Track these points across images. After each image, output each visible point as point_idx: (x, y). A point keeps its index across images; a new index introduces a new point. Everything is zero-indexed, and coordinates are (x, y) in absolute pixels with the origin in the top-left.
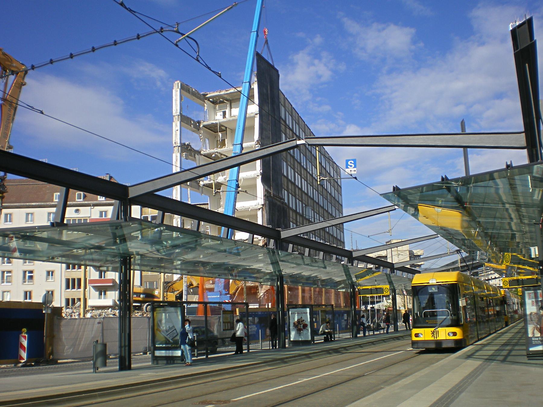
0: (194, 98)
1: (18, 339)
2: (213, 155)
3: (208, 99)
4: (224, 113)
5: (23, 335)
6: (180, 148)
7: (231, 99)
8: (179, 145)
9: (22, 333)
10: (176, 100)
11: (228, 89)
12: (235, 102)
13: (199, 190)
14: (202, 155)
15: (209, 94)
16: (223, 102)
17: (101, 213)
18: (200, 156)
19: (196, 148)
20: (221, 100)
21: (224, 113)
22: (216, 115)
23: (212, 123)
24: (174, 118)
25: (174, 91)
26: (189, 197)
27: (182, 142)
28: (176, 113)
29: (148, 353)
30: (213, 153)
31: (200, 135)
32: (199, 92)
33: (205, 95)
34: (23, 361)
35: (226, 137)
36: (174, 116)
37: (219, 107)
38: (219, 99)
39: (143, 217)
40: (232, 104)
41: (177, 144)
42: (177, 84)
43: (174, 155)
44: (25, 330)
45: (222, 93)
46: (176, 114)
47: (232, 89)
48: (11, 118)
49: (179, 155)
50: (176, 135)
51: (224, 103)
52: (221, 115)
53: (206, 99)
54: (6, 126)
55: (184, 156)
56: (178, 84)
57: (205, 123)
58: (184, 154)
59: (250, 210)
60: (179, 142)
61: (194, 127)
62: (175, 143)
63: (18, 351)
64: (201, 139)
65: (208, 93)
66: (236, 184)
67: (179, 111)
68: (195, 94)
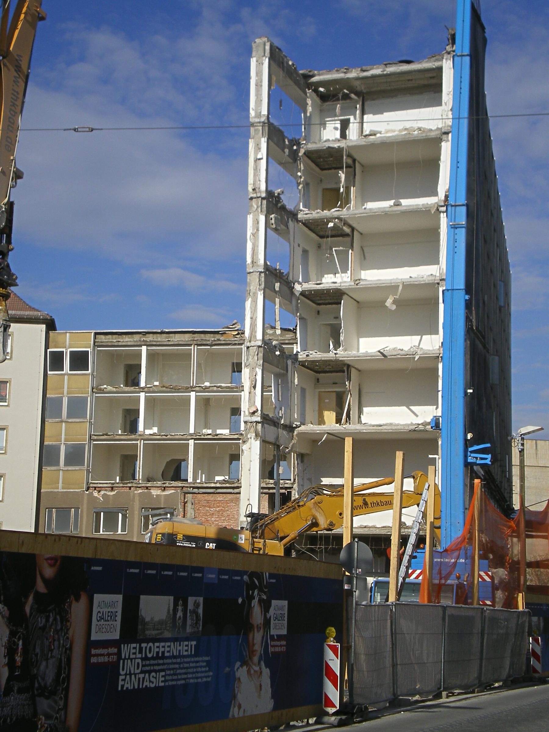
0: (290, 82)
1: (321, 654)
2: (331, 225)
3: (315, 87)
4: (345, 125)
5: (332, 643)
6: (265, 202)
7: (365, 91)
8: (264, 195)
9: (325, 638)
10: (259, 85)
11: (368, 68)
12: (373, 100)
13: (291, 302)
14: (300, 221)
15: (319, 75)
16: (346, 97)
18: (296, 223)
19: (290, 206)
20: (346, 91)
21: (345, 125)
22: (325, 129)
23: (329, 147)
24: (252, 129)
25: (253, 62)
26: (277, 318)
27: (269, 189)
28: (259, 115)
29: (444, 694)
30: (330, 220)
31: (299, 174)
32: (298, 69)
33: (307, 77)
34: (331, 710)
35: (354, 182)
36: (252, 125)
37: (342, 109)
38: (342, 90)
40: (366, 104)
41: (260, 192)
42: (262, 46)
43: (250, 219)
44: (332, 631)
45: (353, 74)
46: (257, 120)
47: (378, 68)
48: (19, 103)
49: (262, 218)
50: (257, 169)
51: (348, 101)
52: (336, 129)
53: (309, 86)
54: (9, 121)
55: (273, 221)
56: (265, 45)
57: (311, 146)
58: (272, 216)
59: (417, 358)
60: (263, 187)
61: (289, 156)
62: (254, 190)
63: (320, 686)
64: (299, 184)
65: (316, 72)
66: (466, 300)
67: (265, 112)
68: (290, 73)
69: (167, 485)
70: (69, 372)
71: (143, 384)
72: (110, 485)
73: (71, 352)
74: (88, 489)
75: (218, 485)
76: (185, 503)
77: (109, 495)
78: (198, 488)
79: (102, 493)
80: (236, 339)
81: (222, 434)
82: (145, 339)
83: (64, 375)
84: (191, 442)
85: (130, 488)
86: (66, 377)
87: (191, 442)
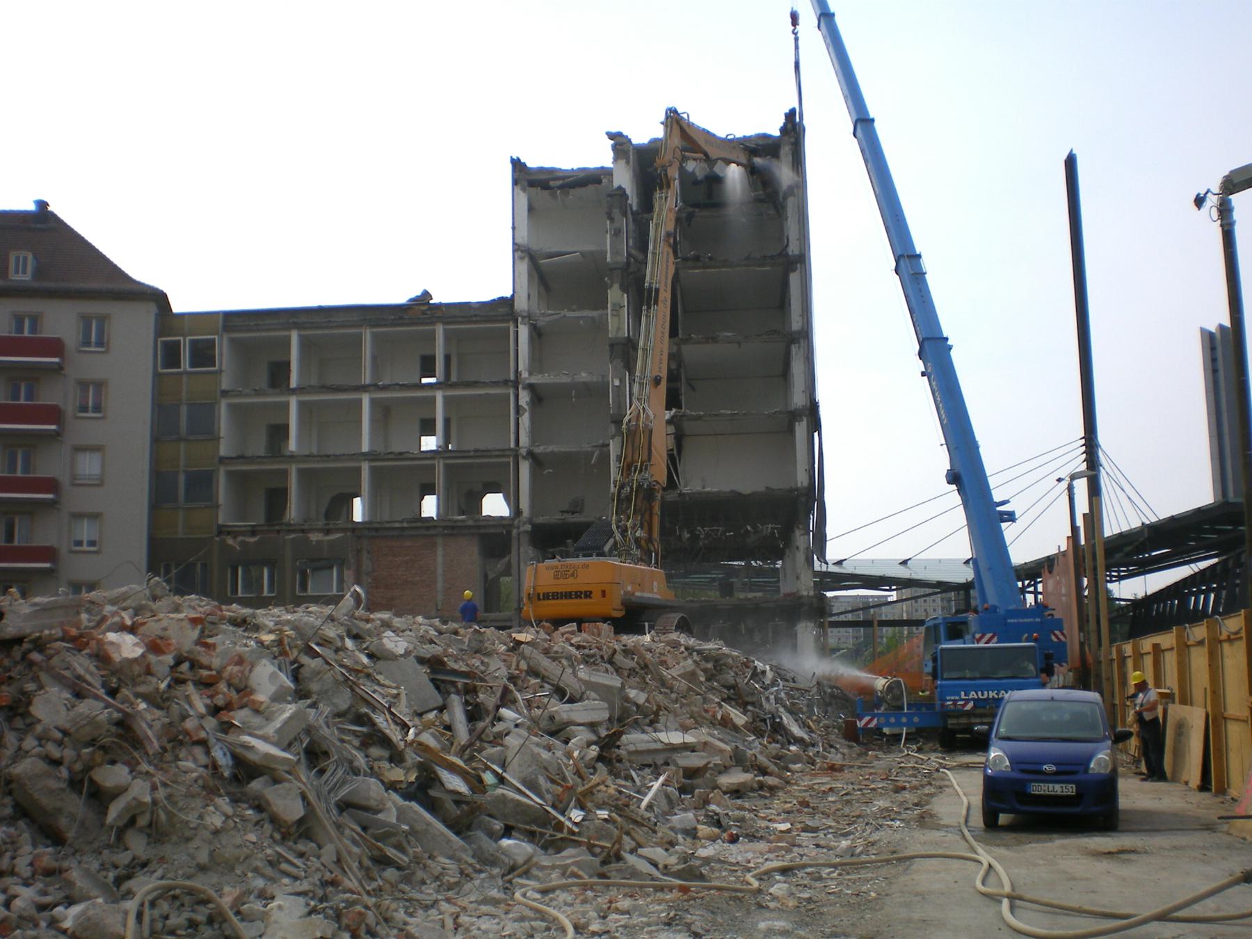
17: (19, 320)
39: (165, 343)
69: (331, 526)
70: (188, 369)
71: (294, 383)
72: (249, 528)
73: (193, 343)
74: (220, 533)
75: (405, 525)
76: (359, 551)
77: (248, 543)
78: (377, 530)
79: (240, 538)
80: (425, 316)
81: (408, 452)
82: (295, 320)
83: (180, 374)
84: (365, 467)
85: (278, 532)
86: (185, 379)
87: (365, 467)
